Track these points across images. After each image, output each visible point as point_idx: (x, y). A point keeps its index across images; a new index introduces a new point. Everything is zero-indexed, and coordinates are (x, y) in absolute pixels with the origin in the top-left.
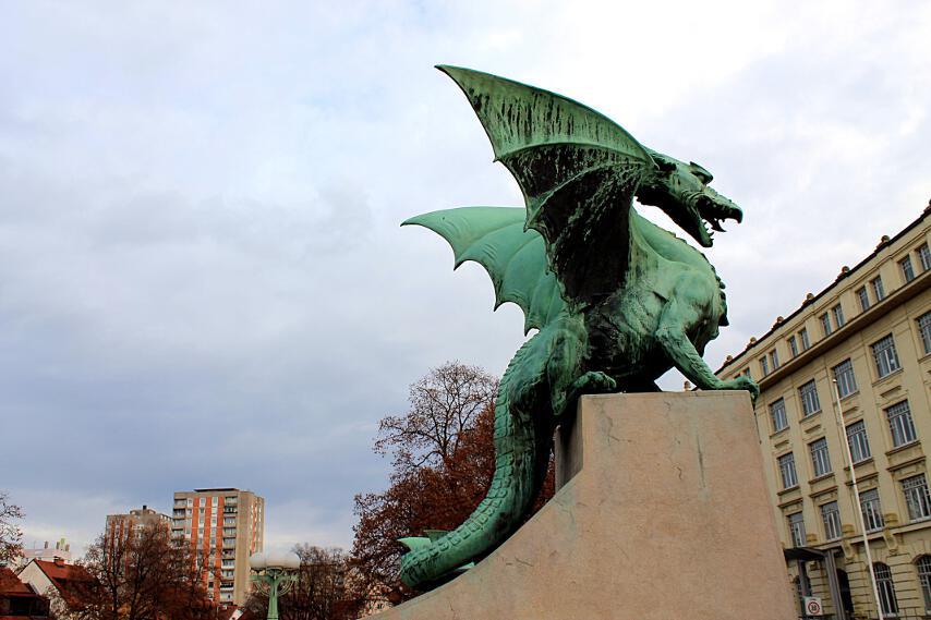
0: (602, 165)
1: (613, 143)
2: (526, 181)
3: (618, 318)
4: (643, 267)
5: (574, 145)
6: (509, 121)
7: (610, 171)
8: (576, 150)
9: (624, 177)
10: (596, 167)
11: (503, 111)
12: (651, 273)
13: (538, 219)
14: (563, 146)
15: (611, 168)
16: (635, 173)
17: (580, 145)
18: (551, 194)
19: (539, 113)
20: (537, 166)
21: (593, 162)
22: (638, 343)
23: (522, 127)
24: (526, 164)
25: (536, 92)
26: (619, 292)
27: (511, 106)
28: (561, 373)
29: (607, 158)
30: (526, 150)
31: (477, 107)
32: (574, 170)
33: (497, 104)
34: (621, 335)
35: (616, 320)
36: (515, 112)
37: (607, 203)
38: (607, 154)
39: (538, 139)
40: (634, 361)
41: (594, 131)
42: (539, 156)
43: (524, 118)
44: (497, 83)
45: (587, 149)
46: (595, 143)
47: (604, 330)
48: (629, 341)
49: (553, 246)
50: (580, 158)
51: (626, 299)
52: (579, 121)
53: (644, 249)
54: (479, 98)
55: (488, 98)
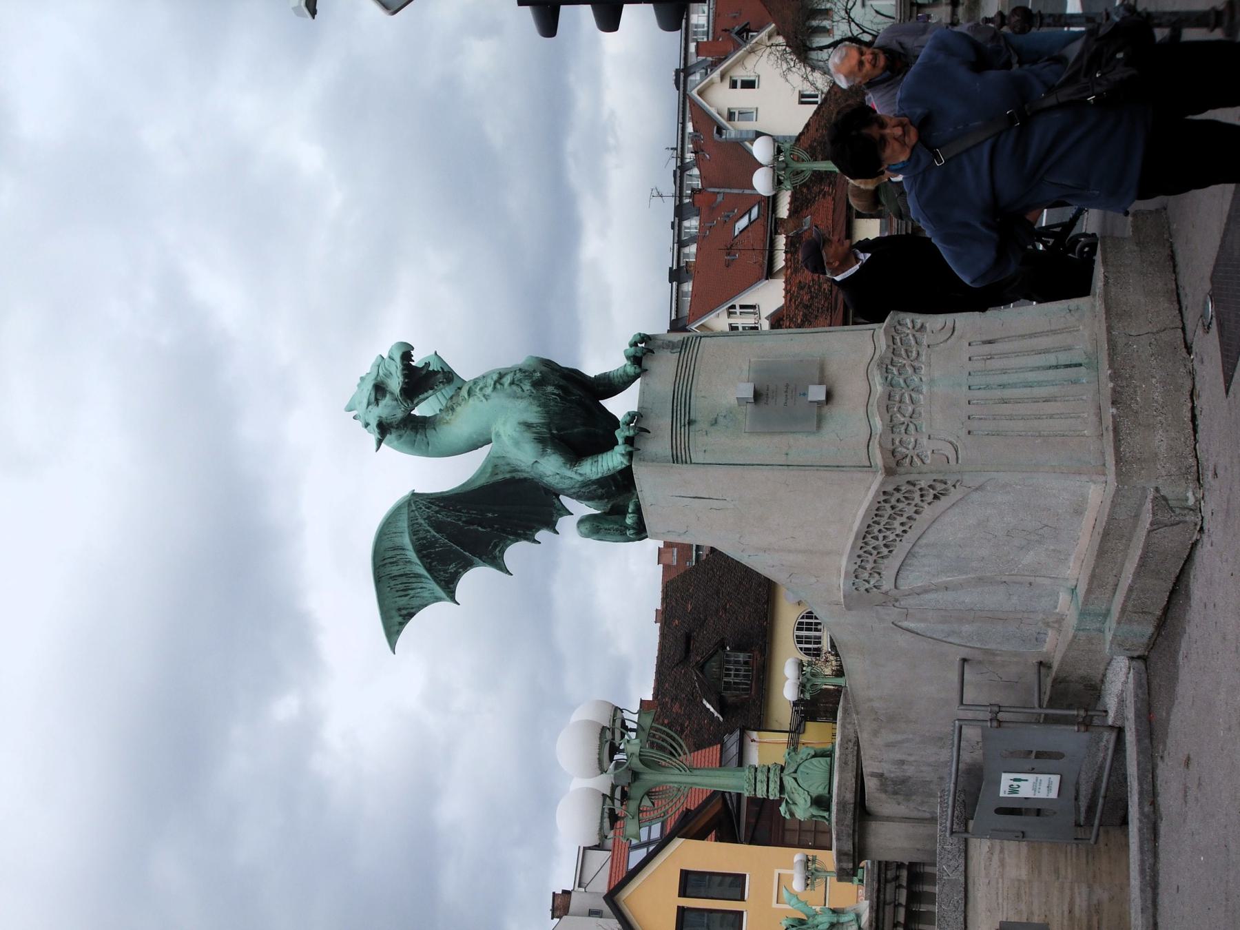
1: (399, 524)
4: (508, 468)
7: (428, 518)
12: (514, 462)
19: (395, 570)
23: (413, 580)
24: (445, 571)
25: (378, 580)
30: (436, 579)
31: (411, 615)
36: (402, 587)
39: (422, 570)
43: (404, 579)
52: (388, 544)
53: (490, 470)
55: (399, 609)
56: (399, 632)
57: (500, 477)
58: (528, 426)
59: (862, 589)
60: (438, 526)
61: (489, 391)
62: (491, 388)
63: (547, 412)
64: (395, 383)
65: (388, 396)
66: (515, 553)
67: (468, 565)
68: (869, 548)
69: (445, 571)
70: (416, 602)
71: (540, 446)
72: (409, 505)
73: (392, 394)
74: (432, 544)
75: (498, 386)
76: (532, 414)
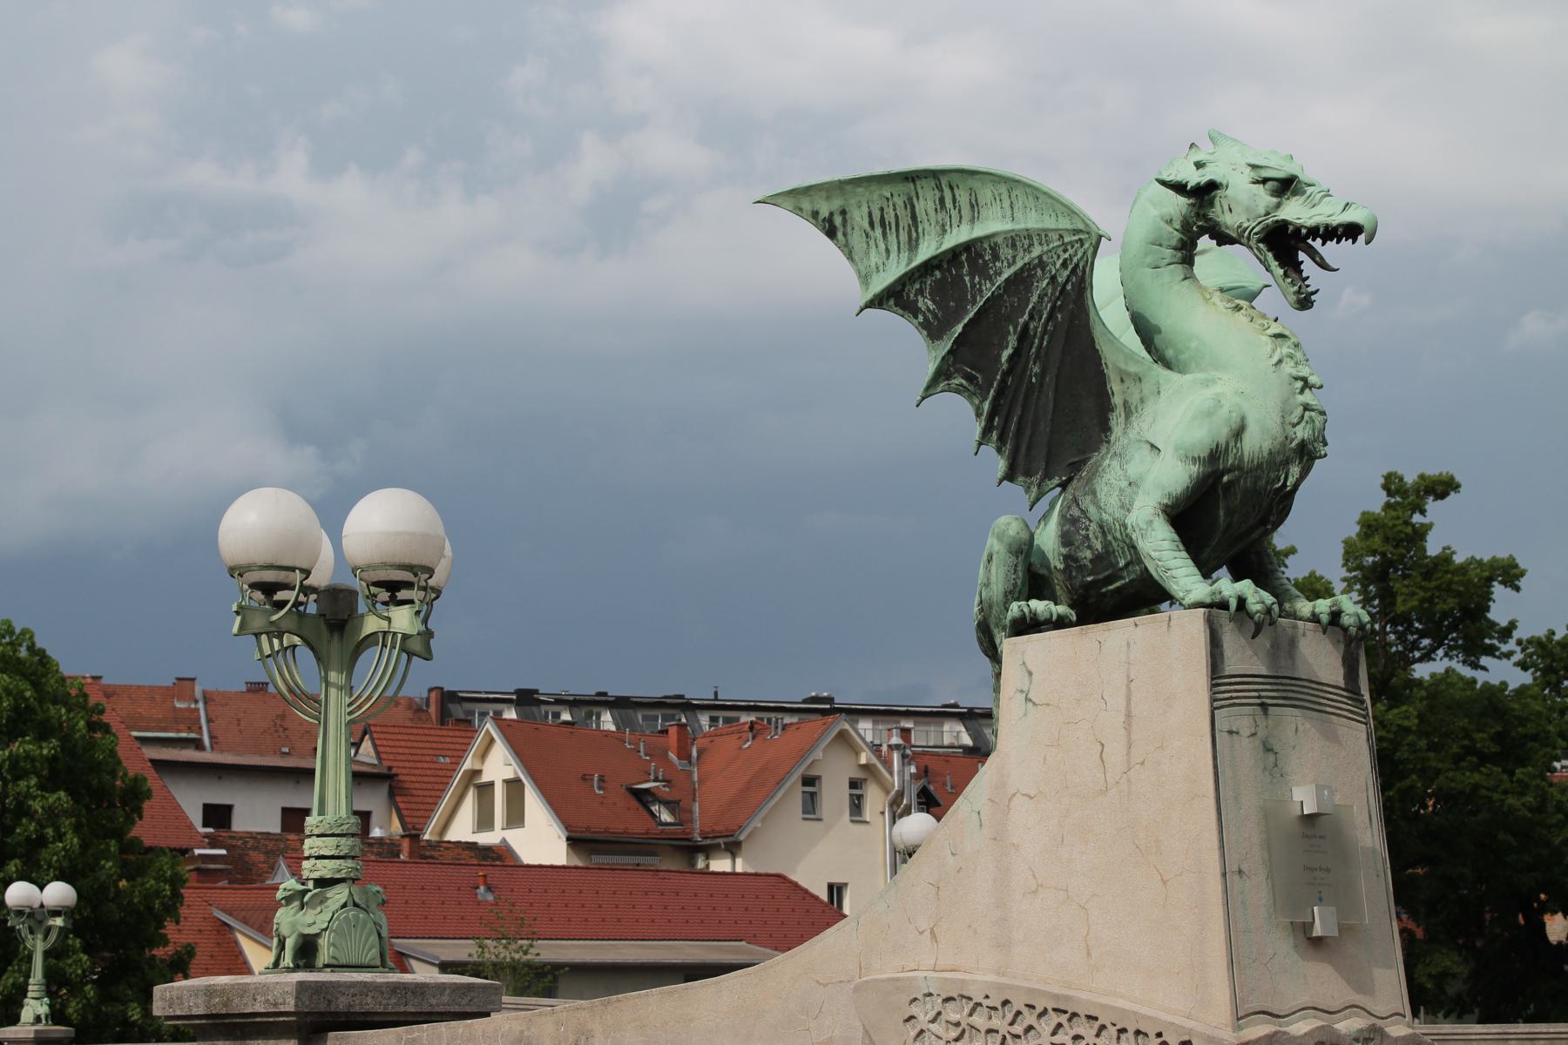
0: (1026, 260)
2: (926, 318)
3: (1089, 498)
4: (1134, 400)
5: (980, 240)
6: (884, 235)
7: (1042, 264)
8: (986, 245)
9: (1064, 265)
10: (1019, 264)
11: (872, 224)
12: (1149, 410)
13: (942, 375)
14: (968, 247)
15: (1040, 257)
16: (1080, 254)
17: (988, 237)
18: (959, 328)
20: (939, 292)
21: (1014, 257)
22: (1118, 535)
23: (904, 237)
26: (1103, 449)
27: (882, 209)
28: (990, 607)
29: (1031, 245)
31: (831, 233)
32: (990, 278)
33: (859, 218)
34: (1093, 527)
35: (1086, 502)
37: (1051, 316)
38: (1030, 237)
39: (926, 251)
40: (1122, 563)
41: (1006, 204)
42: (938, 274)
44: (849, 188)
45: (1000, 240)
46: (1008, 226)
47: (1074, 521)
48: (1104, 533)
49: (986, 406)
50: (996, 257)
51: (1107, 462)
52: (986, 193)
53: (1132, 369)
54: (830, 219)
55: (843, 212)
56: (798, 210)
57: (1114, 385)
58: (1239, 433)
59: (914, 1010)
60: (1022, 281)
61: (1288, 368)
62: (1294, 372)
63: (1260, 466)
64: (1295, 211)
65: (1275, 200)
66: (959, 415)
67: (934, 331)
68: (1029, 1018)
69: (920, 292)
70: (857, 240)
71: (1204, 454)
72: (1076, 232)
73: (1278, 206)
74: (980, 269)
75: (1299, 384)
76: (1256, 443)
